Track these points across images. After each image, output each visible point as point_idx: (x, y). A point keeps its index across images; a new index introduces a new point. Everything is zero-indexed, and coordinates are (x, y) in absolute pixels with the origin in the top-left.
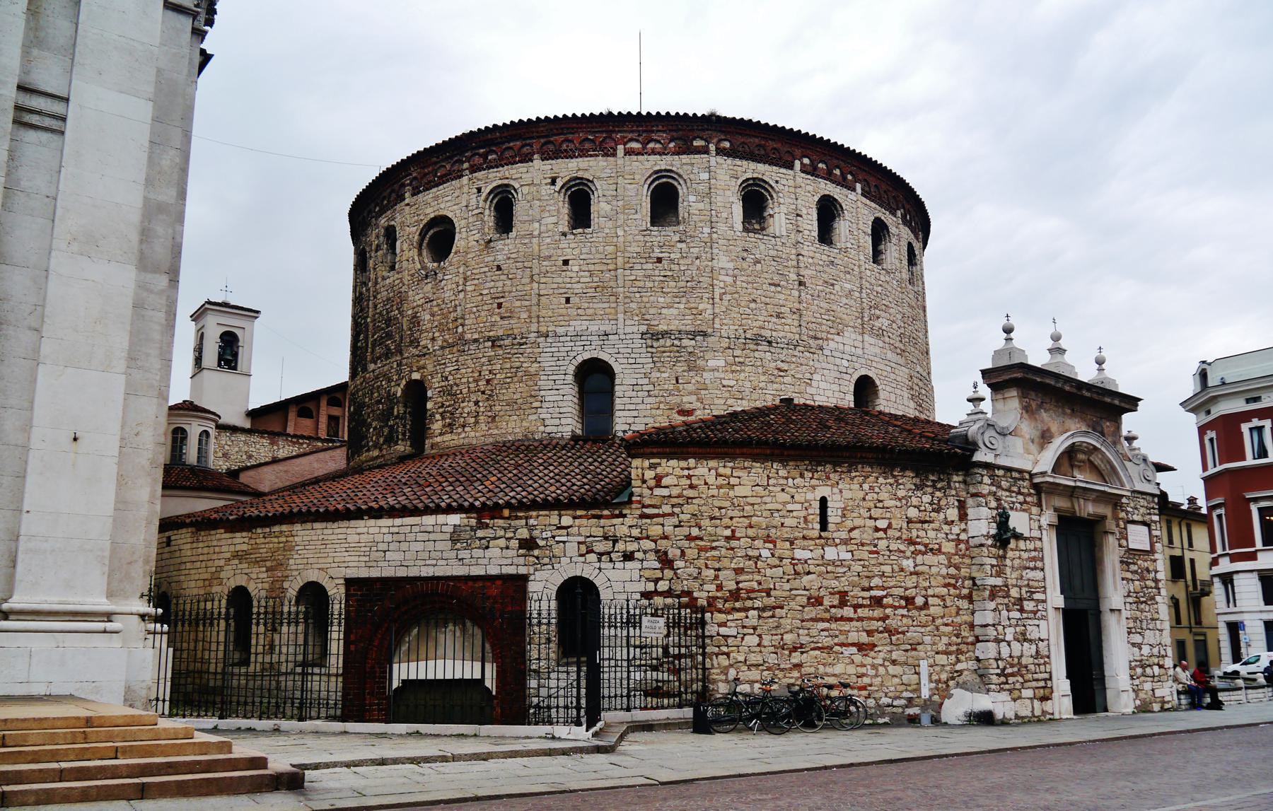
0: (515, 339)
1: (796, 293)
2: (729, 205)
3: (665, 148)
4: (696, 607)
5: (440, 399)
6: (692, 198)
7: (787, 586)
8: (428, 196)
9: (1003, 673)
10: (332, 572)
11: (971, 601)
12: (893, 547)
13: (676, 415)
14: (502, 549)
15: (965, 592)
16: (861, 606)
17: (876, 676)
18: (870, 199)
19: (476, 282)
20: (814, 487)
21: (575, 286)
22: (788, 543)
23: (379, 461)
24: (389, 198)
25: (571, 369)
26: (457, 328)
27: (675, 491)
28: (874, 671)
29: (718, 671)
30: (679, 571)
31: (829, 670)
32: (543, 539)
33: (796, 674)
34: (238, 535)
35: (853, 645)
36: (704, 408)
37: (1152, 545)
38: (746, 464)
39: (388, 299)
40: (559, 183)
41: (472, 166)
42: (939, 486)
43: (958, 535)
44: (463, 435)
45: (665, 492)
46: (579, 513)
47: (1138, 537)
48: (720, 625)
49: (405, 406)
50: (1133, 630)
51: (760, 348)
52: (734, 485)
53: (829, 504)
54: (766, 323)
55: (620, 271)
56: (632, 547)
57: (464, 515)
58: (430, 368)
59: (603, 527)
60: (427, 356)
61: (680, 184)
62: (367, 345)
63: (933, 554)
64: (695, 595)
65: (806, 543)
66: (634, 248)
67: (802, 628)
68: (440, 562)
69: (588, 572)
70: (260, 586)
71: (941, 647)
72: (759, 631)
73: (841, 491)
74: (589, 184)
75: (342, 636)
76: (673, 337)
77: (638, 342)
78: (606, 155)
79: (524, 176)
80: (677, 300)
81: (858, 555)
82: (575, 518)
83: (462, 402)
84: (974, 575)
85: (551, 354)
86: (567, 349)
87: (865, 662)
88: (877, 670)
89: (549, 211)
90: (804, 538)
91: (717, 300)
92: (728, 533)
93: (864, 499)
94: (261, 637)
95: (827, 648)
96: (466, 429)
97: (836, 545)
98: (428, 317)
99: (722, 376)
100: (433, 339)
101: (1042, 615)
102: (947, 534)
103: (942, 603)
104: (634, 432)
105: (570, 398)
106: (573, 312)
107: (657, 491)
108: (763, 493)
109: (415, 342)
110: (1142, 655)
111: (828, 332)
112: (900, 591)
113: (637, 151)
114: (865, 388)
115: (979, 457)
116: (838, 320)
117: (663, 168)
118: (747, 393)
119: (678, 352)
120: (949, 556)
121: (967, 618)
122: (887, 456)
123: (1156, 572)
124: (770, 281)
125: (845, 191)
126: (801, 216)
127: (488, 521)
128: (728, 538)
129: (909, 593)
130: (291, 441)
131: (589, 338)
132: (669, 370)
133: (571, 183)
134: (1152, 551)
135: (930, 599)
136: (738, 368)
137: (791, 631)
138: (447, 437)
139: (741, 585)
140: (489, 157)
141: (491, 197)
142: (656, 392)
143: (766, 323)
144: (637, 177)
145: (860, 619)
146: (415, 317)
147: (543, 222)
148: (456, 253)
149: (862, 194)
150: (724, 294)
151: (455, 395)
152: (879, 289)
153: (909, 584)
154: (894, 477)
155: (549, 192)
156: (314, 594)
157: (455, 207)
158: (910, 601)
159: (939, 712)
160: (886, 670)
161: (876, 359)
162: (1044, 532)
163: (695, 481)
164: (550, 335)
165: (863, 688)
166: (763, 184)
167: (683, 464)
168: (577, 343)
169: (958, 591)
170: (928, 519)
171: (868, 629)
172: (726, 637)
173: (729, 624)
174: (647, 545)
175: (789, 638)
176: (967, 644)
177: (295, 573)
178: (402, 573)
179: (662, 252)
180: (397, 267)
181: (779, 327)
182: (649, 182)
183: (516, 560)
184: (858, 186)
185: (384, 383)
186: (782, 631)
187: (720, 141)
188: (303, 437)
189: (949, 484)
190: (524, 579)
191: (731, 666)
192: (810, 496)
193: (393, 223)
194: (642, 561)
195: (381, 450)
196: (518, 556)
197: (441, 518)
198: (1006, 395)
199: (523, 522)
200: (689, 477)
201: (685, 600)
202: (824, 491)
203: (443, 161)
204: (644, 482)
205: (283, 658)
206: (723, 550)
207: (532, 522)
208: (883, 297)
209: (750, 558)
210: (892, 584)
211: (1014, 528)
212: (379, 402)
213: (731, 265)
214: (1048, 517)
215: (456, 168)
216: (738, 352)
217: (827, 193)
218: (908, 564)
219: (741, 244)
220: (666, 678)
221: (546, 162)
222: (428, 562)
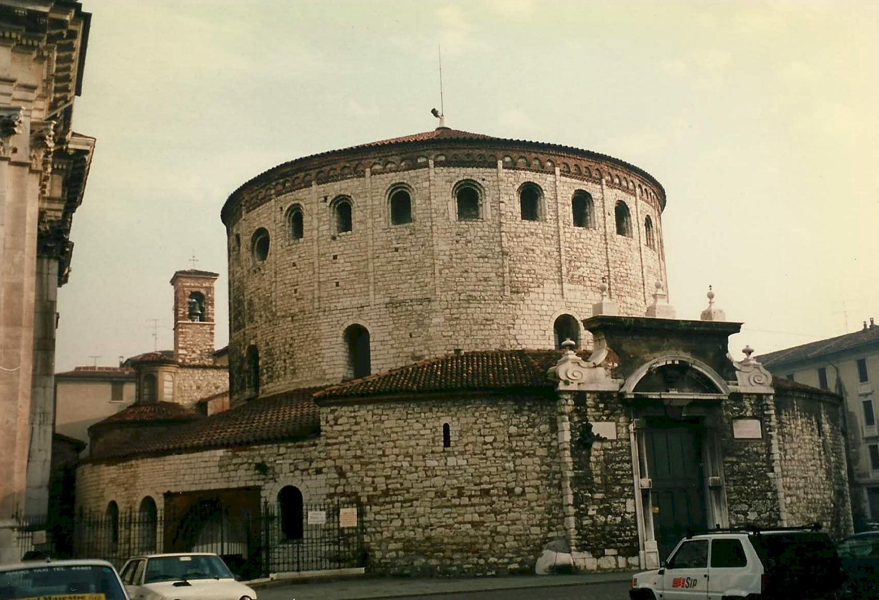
3: (398, 167)
7: (421, 485)
8: (253, 214)
12: (498, 454)
15: (556, 482)
16: (473, 496)
17: (485, 543)
18: (570, 177)
19: (281, 275)
20: (439, 418)
21: (342, 274)
25: (341, 333)
27: (346, 427)
35: (469, 523)
38: (392, 406)
40: (329, 200)
42: (534, 409)
43: (550, 443)
44: (278, 384)
45: (340, 428)
46: (290, 445)
48: (376, 514)
51: (471, 305)
52: (384, 421)
53: (450, 429)
56: (321, 465)
57: (225, 450)
58: (259, 337)
63: (529, 457)
64: (359, 494)
67: (431, 513)
68: (213, 481)
69: (296, 483)
72: (402, 516)
73: (458, 419)
77: (384, 310)
78: (359, 177)
81: (471, 461)
82: (288, 448)
88: (486, 539)
91: (437, 274)
92: (380, 452)
93: (476, 423)
94: (123, 533)
95: (449, 525)
96: (280, 379)
97: (456, 456)
98: (257, 300)
99: (442, 329)
100: (261, 316)
101: (628, 495)
103: (536, 491)
105: (340, 353)
106: (341, 292)
107: (336, 428)
109: (251, 319)
112: (504, 485)
113: (379, 171)
116: (539, 276)
124: (479, 255)
128: (380, 456)
135: (526, 488)
136: (455, 322)
137: (424, 515)
138: (270, 385)
142: (397, 345)
145: (473, 505)
147: (321, 229)
151: (273, 355)
152: (580, 246)
153: (510, 479)
154: (498, 406)
158: (510, 491)
160: (493, 539)
163: (358, 420)
167: (351, 409)
172: (380, 521)
174: (330, 463)
175: (422, 521)
177: (139, 491)
179: (398, 244)
182: (388, 193)
190: (259, 489)
192: (436, 424)
197: (213, 452)
199: (257, 452)
200: (354, 417)
201: (353, 497)
202: (446, 420)
204: (327, 422)
208: (584, 251)
209: (395, 468)
211: (598, 435)
213: (448, 248)
216: (454, 311)
221: (320, 186)
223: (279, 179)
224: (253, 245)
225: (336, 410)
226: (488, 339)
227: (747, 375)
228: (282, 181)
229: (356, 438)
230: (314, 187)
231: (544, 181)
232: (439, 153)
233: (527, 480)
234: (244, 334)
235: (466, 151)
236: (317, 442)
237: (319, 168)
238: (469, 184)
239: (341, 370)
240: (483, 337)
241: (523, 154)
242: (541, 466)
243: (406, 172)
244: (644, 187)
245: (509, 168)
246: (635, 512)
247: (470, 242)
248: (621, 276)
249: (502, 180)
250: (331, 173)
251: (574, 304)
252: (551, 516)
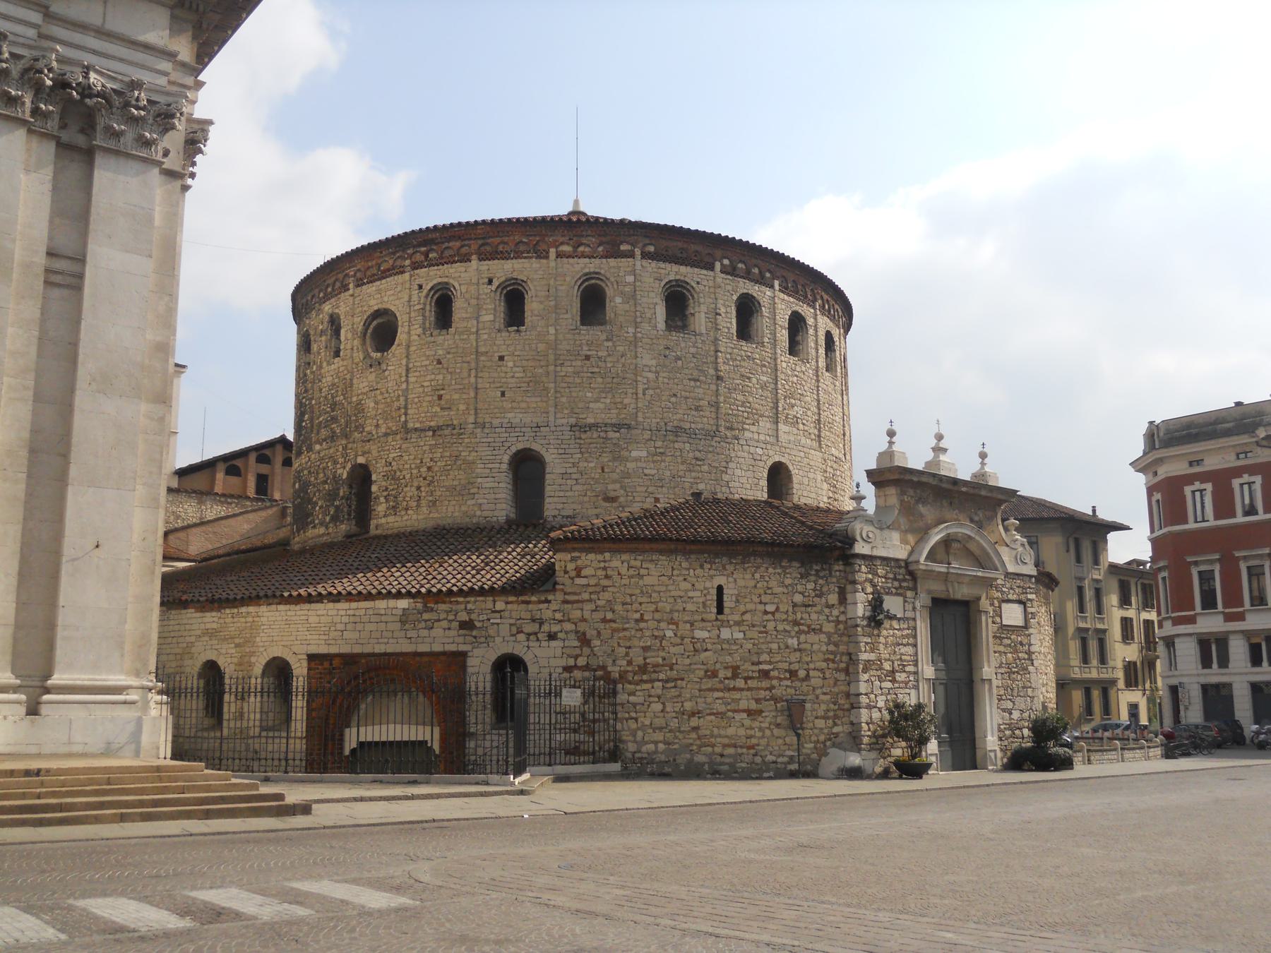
0: (454, 429)
1: (713, 387)
2: (652, 306)
4: (610, 679)
5: (384, 483)
6: (618, 300)
7: (687, 661)
10: (295, 649)
11: (847, 671)
12: (780, 627)
13: (602, 502)
14: (444, 629)
15: (843, 665)
17: (763, 737)
19: (417, 374)
20: (712, 577)
21: (510, 380)
22: (688, 625)
23: (325, 538)
24: (334, 286)
25: (506, 458)
26: (400, 416)
27: (592, 582)
28: (761, 734)
29: (628, 733)
30: (595, 649)
31: (722, 732)
32: (479, 621)
33: (694, 735)
34: (208, 614)
35: (744, 711)
36: (627, 496)
37: (1026, 620)
39: (333, 385)
41: (413, 263)
43: (837, 617)
44: (406, 518)
46: (511, 599)
47: (1013, 615)
49: (351, 487)
50: (1004, 697)
52: (643, 576)
53: (725, 592)
54: (686, 416)
55: (551, 368)
56: (555, 628)
57: (412, 600)
58: (375, 453)
59: (531, 611)
60: (371, 442)
61: (607, 285)
62: (312, 426)
65: (704, 624)
66: (564, 346)
67: (700, 697)
68: (391, 641)
69: (519, 650)
70: (229, 660)
71: (821, 713)
73: (735, 580)
74: (523, 284)
75: (305, 704)
76: (599, 430)
77: (567, 435)
78: (539, 257)
79: (463, 275)
80: (604, 395)
81: (749, 635)
82: (507, 603)
83: (406, 486)
84: (851, 651)
85: (487, 444)
86: (502, 440)
87: (754, 726)
88: (764, 732)
89: (486, 310)
90: (703, 620)
91: (640, 395)
92: (637, 616)
93: (755, 586)
94: (233, 705)
95: (721, 713)
96: (409, 512)
97: (730, 627)
98: (372, 405)
99: (644, 465)
100: (377, 426)
102: (828, 616)
103: (822, 676)
104: (563, 517)
106: (508, 405)
107: (578, 581)
108: (668, 582)
109: (359, 428)
110: (1011, 719)
111: (744, 423)
112: (785, 666)
113: (568, 254)
114: (778, 476)
117: (592, 270)
118: (667, 481)
119: (604, 443)
120: (829, 635)
121: (844, 688)
122: (776, 549)
123: (1030, 645)
124: (690, 377)
125: (763, 288)
126: (720, 315)
127: (433, 606)
128: (637, 621)
129: (795, 667)
130: (220, 501)
131: (523, 430)
132: (595, 460)
133: (507, 283)
134: (1026, 627)
136: (659, 458)
138: (391, 519)
139: (648, 661)
140: (430, 256)
141: (432, 293)
143: (686, 416)
144: (568, 279)
146: (360, 403)
147: (482, 319)
148: (399, 345)
149: (780, 290)
150: (647, 389)
151: (399, 479)
153: (793, 660)
154: (782, 567)
155: (486, 291)
156: (279, 671)
157: (397, 302)
158: (793, 674)
159: (817, 768)
160: (772, 732)
161: (790, 446)
162: (918, 614)
163: (610, 572)
164: (487, 425)
165: (752, 747)
166: (684, 285)
167: (600, 557)
168: (511, 435)
169: (836, 665)
170: (811, 603)
171: (756, 697)
172: (635, 705)
173: (638, 693)
174: (568, 626)
175: (688, 706)
176: (843, 710)
177: (261, 649)
178: (357, 649)
179: (589, 350)
180: (341, 354)
181: (698, 419)
182: (579, 283)
183: (457, 640)
184: (776, 283)
185: (329, 464)
186: (683, 699)
187: (645, 245)
188: (232, 496)
189: (830, 573)
190: (464, 655)
191: (638, 729)
192: (708, 584)
193: (337, 311)
194: (564, 640)
195: (327, 528)
196: (459, 636)
197: (392, 603)
198: (887, 493)
199: (463, 606)
200: (605, 569)
201: (599, 673)
203: (385, 256)
204: (566, 572)
205: (251, 724)
206: (633, 632)
207: (469, 606)
209: (656, 637)
210: (778, 659)
211: (888, 610)
212: (325, 482)
213: (654, 362)
214: (923, 600)
215: (398, 263)
217: (745, 291)
218: (793, 642)
219: (663, 342)
220: (582, 739)
221: (483, 262)
222: (380, 641)
223: (420, 245)
224: (366, 330)
225: (580, 557)
226: (697, 483)
227: (1014, 552)
228: (423, 249)
229: (607, 595)
230: (474, 262)
231: (763, 294)
232: (648, 242)
233: (811, 662)
234: (345, 448)
235: (680, 244)
236: (550, 597)
237: (483, 238)
238: (679, 286)
239: (504, 506)
240: (692, 480)
241: (743, 259)
242: (827, 644)
243: (604, 260)
245: (728, 273)
247: (680, 359)
248: (829, 423)
249: (720, 287)
250: (500, 248)
251: (788, 450)
252: (836, 707)
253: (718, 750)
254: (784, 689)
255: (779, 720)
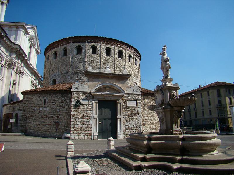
9: (75, 130)
18: (105, 44)
90: (41, 106)
93: (52, 99)
115: (72, 90)
120: (66, 109)
123: (138, 110)
129: (58, 115)
145: (49, 120)
154: (57, 95)
158: (58, 117)
162: (93, 104)
165: (49, 132)
167: (27, 95)
172: (30, 122)
175: (38, 123)
189: (68, 96)
192: (43, 99)
202: (45, 98)
231: (98, 45)
244: (129, 48)
246: (92, 124)
253: (42, 132)
254: (56, 120)
255: (54, 126)
